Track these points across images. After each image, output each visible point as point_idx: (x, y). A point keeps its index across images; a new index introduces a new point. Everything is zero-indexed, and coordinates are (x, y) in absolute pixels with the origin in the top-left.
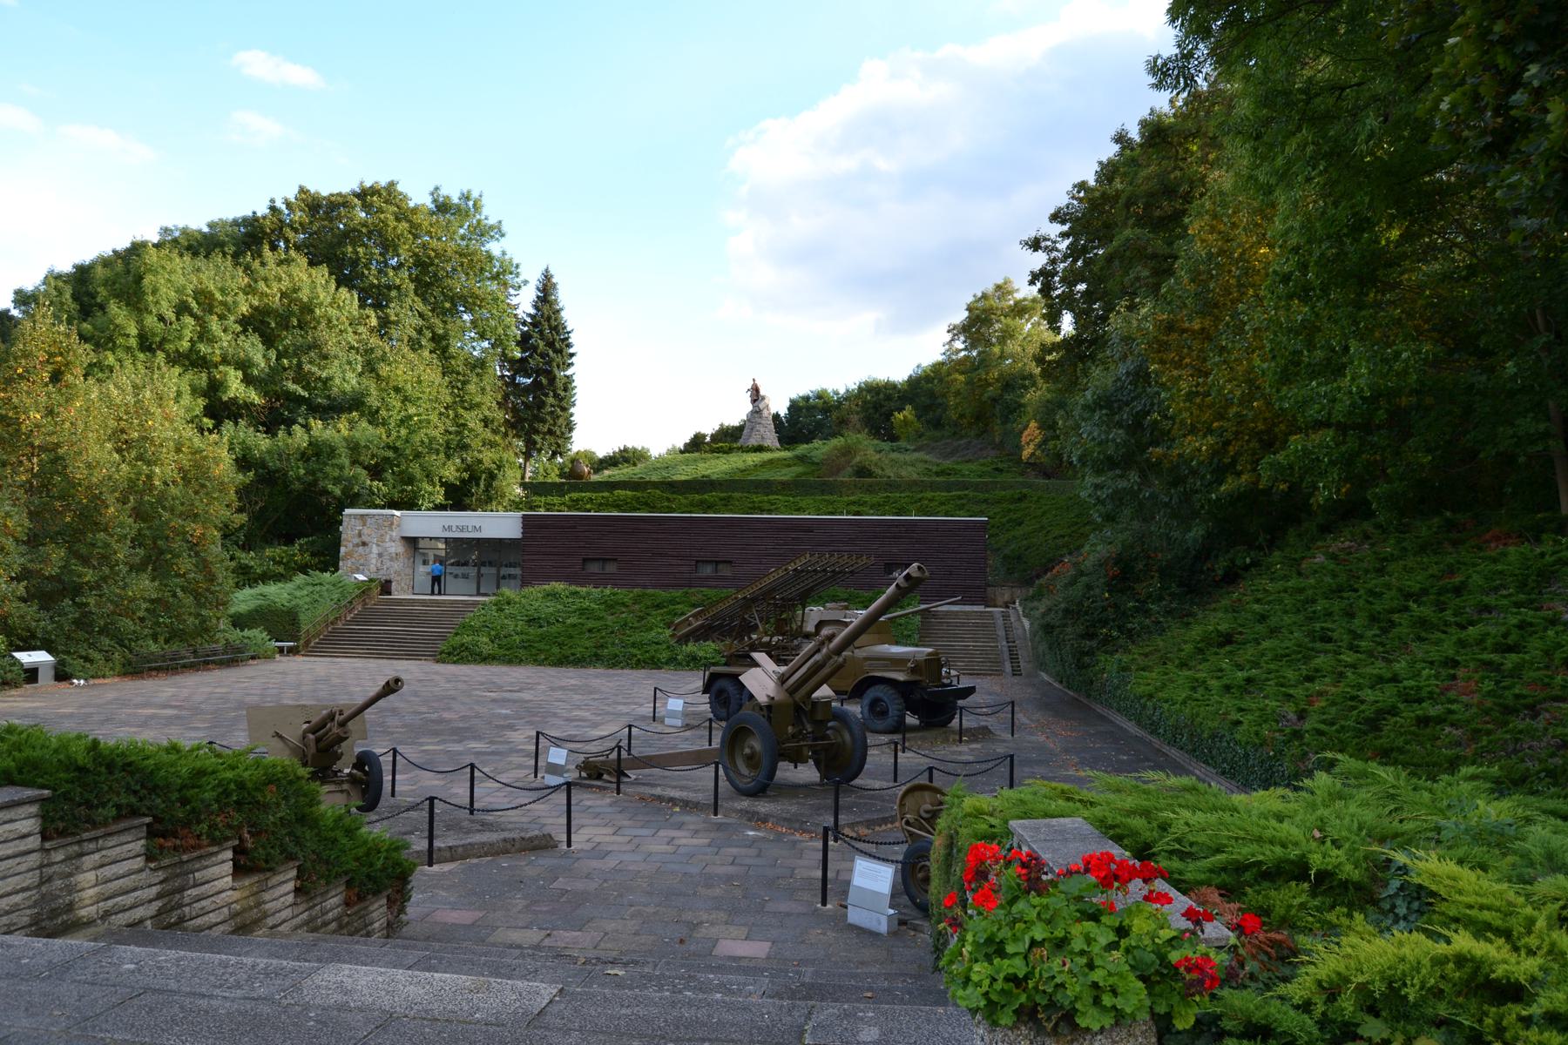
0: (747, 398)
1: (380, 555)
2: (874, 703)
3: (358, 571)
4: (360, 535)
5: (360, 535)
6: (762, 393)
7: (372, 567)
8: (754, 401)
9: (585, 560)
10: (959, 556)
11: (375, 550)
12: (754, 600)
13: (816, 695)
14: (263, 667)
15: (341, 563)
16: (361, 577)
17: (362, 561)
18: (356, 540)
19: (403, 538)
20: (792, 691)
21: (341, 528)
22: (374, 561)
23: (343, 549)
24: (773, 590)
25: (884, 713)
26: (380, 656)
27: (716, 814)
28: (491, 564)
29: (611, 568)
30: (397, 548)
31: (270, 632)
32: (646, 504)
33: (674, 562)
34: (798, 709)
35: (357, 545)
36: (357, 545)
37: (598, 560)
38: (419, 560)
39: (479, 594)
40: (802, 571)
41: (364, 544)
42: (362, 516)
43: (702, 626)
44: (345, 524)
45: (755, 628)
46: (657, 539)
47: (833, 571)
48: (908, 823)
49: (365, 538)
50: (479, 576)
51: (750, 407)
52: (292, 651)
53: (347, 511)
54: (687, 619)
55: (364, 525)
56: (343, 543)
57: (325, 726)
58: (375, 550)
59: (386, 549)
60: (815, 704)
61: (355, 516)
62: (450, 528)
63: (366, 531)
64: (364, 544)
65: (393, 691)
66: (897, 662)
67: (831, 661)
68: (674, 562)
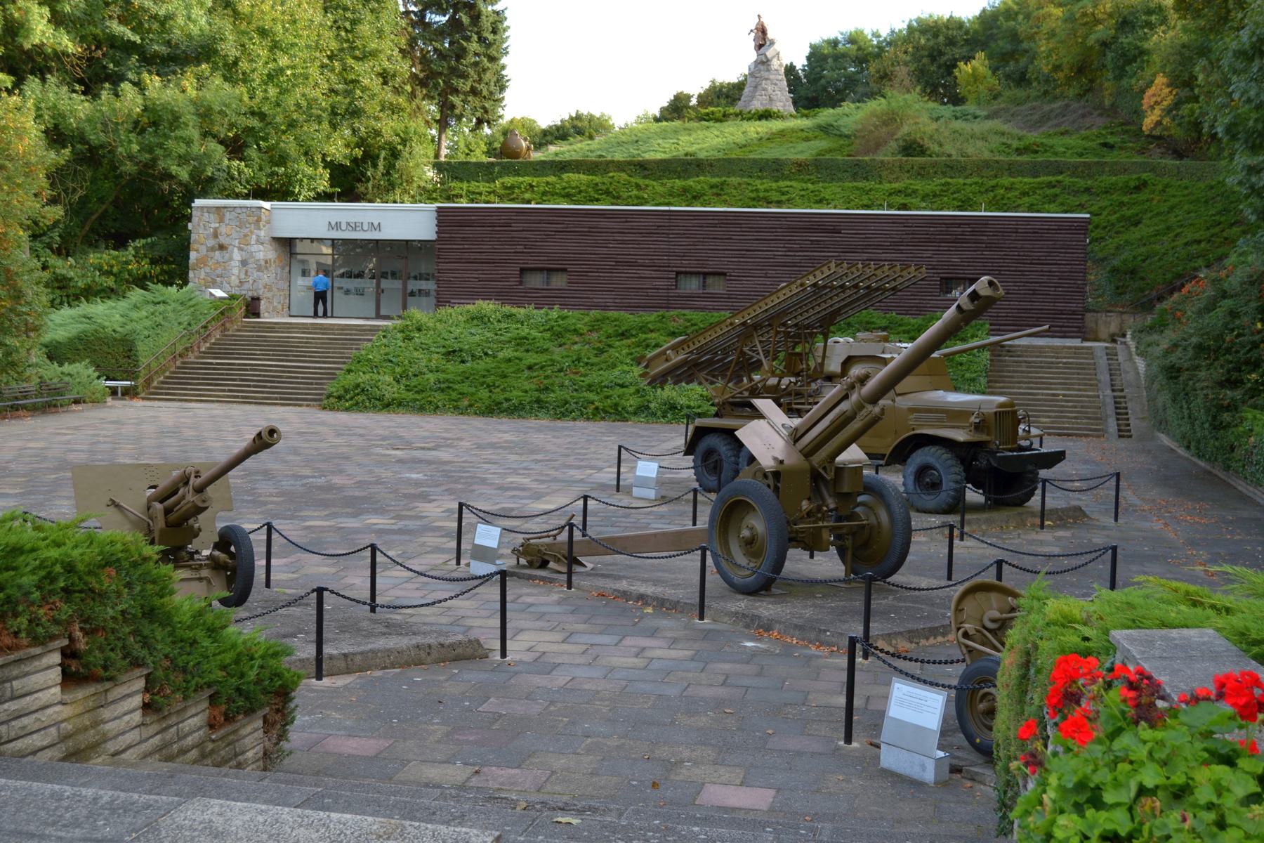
0: (750, 43)
1: (244, 263)
2: (922, 471)
3: (214, 284)
4: (216, 235)
5: (216, 235)
6: (770, 35)
7: (234, 280)
8: (759, 47)
9: (522, 270)
10: (1046, 268)
11: (237, 256)
12: (756, 327)
13: (841, 458)
14: (86, 414)
15: (191, 274)
16: (219, 293)
17: (219, 271)
18: (211, 242)
19: (274, 239)
20: (808, 453)
21: (190, 226)
22: (235, 271)
23: (193, 255)
24: (784, 312)
25: (935, 486)
26: (246, 400)
27: (702, 617)
28: (394, 275)
29: (559, 281)
30: (264, 252)
31: (98, 367)
32: (608, 193)
33: (647, 273)
34: (816, 477)
35: (212, 249)
36: (212, 249)
37: (541, 270)
38: (297, 269)
39: (378, 316)
40: (825, 287)
41: (222, 247)
42: (218, 208)
43: (684, 363)
44: (195, 219)
45: (757, 366)
46: (623, 242)
47: (868, 287)
48: (966, 635)
49: (222, 240)
50: (379, 292)
51: (753, 56)
52: (129, 393)
53: (198, 202)
54: (664, 353)
55: (221, 221)
56: (193, 246)
57: (175, 492)
58: (237, 256)
59: (251, 255)
60: (839, 471)
61: (209, 209)
62: (338, 225)
63: (223, 230)
64: (222, 247)
65: (268, 446)
66: (955, 415)
67: (864, 412)
68: (647, 273)
